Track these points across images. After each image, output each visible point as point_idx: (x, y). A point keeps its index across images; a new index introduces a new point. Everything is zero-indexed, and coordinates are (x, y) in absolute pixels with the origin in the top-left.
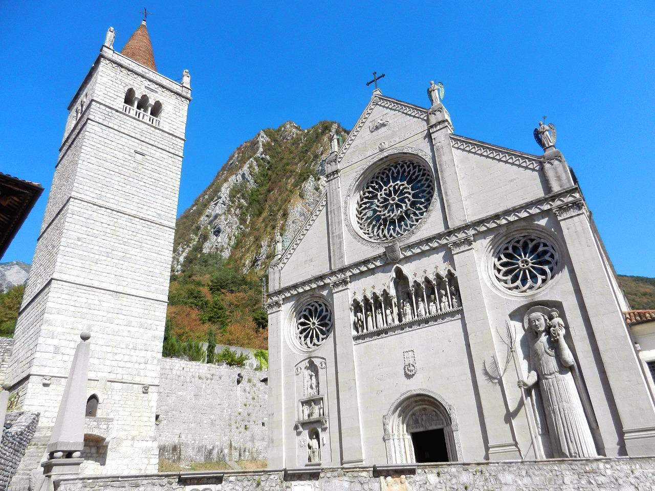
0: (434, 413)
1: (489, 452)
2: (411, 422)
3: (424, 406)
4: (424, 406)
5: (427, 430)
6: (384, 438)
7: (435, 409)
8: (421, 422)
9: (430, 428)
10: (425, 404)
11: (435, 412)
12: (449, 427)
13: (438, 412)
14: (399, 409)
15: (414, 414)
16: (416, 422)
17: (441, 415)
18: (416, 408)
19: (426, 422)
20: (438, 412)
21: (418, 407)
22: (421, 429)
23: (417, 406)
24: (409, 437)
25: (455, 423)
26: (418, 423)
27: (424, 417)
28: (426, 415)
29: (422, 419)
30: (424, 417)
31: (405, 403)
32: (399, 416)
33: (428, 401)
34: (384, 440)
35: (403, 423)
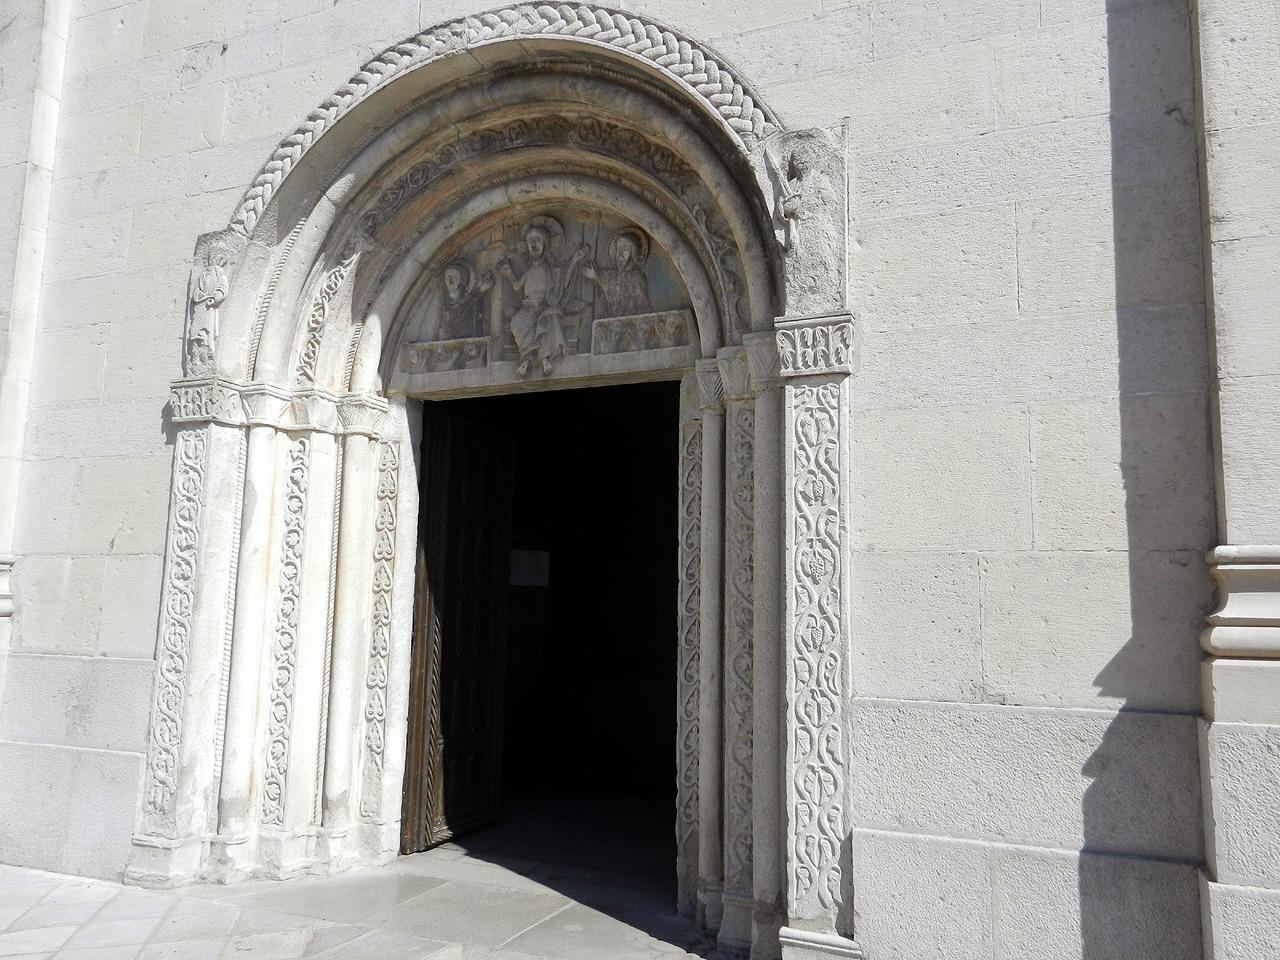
0: (624, 248)
1: (1219, 636)
2: (428, 318)
3: (552, 190)
4: (552, 190)
5: (534, 384)
6: (168, 411)
7: (635, 213)
8: (506, 320)
9: (573, 370)
10: (566, 172)
11: (637, 236)
12: (752, 343)
13: (662, 236)
14: (339, 189)
15: (454, 257)
16: (468, 317)
17: (680, 260)
18: (478, 206)
19: (540, 318)
20: (662, 236)
21: (498, 198)
22: (494, 377)
23: (502, 180)
24: (397, 424)
25: (818, 306)
26: (481, 329)
27: (535, 284)
28: (549, 262)
29: (517, 302)
30: (535, 284)
31: (393, 142)
32: (331, 250)
33: (599, 135)
34: (172, 428)
35: (360, 315)
